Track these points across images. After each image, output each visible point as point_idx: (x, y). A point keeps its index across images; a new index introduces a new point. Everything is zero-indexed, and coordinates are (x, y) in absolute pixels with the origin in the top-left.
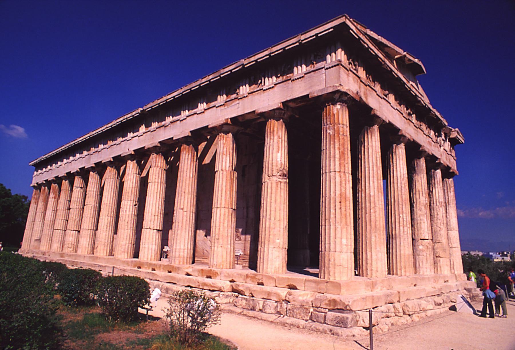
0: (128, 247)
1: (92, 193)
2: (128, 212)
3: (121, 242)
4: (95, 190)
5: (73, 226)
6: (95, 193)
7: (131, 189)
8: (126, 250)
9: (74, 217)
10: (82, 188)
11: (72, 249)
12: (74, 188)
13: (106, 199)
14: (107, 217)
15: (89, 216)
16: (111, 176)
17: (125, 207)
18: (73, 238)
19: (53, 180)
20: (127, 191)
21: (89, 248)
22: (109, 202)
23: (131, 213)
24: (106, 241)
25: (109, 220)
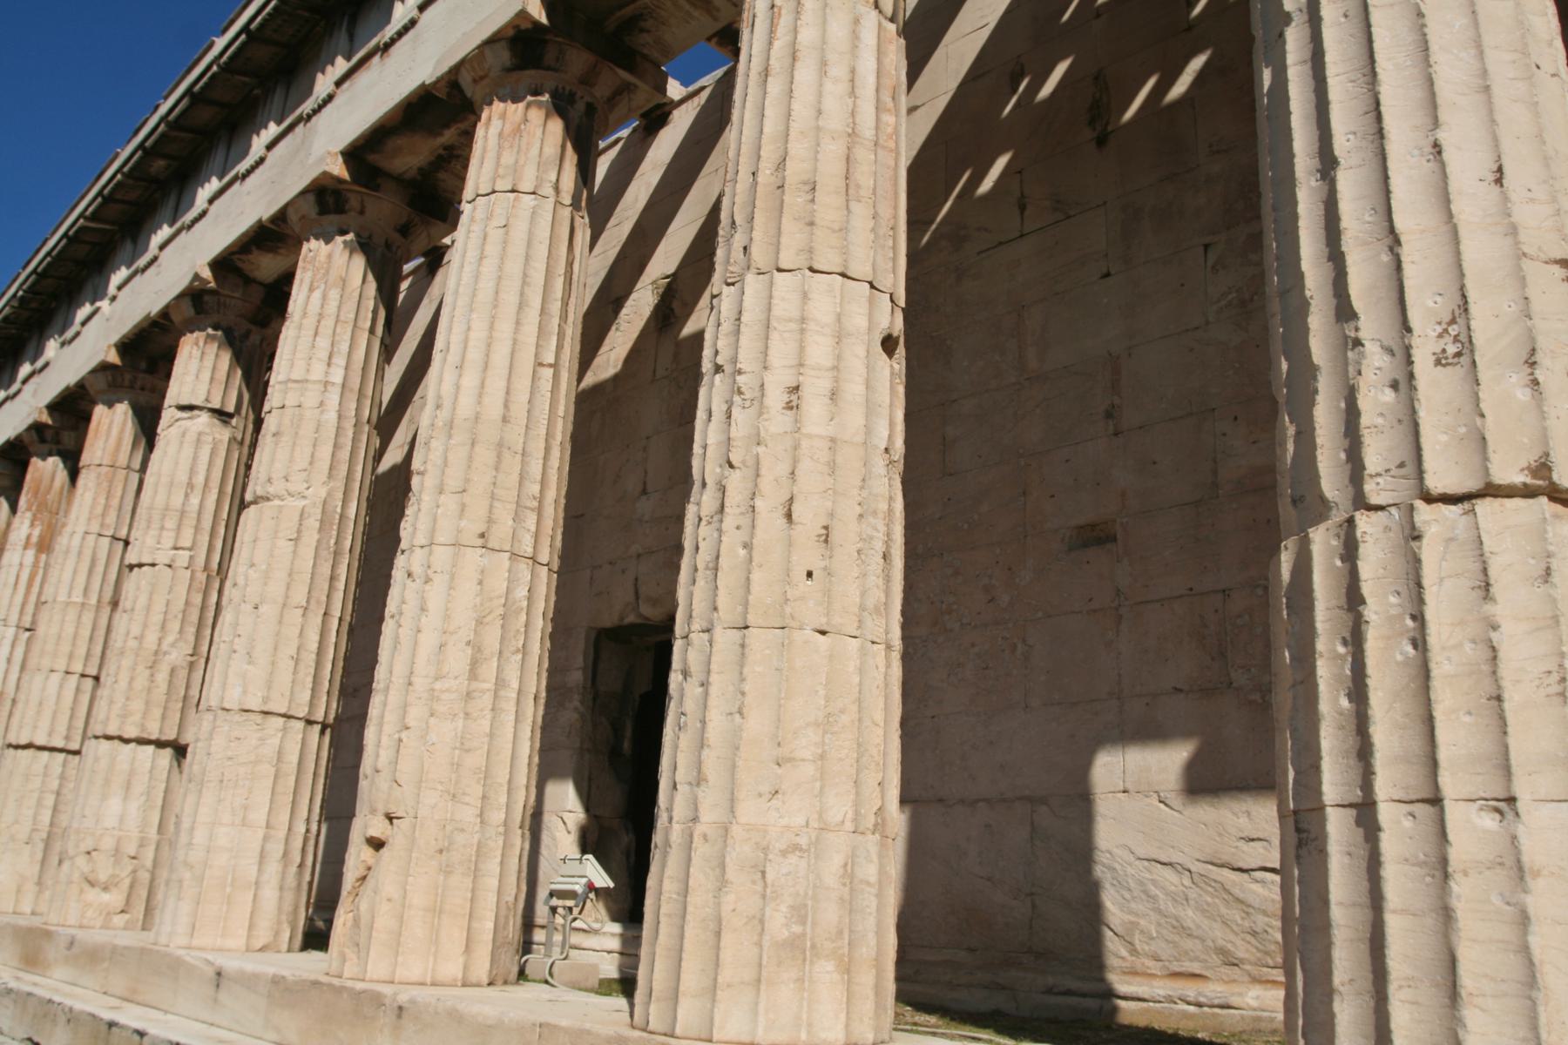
0: (849, 874)
1: (311, 399)
2: (814, 406)
3: (748, 810)
4: (337, 376)
5: (137, 706)
6: (334, 398)
7: (833, 150)
8: (830, 914)
9: (151, 639)
10: (222, 415)
11: (115, 898)
12: (168, 414)
13: (470, 381)
14: (474, 558)
15: (276, 589)
16: (516, 170)
17: (781, 351)
18: (134, 807)
19: (37, 428)
20: (796, 170)
21: (270, 894)
22: (494, 408)
23: (854, 419)
24: (468, 815)
25: (499, 584)
